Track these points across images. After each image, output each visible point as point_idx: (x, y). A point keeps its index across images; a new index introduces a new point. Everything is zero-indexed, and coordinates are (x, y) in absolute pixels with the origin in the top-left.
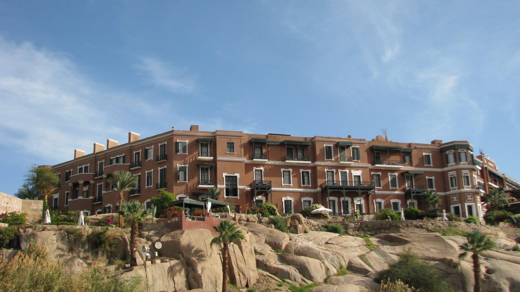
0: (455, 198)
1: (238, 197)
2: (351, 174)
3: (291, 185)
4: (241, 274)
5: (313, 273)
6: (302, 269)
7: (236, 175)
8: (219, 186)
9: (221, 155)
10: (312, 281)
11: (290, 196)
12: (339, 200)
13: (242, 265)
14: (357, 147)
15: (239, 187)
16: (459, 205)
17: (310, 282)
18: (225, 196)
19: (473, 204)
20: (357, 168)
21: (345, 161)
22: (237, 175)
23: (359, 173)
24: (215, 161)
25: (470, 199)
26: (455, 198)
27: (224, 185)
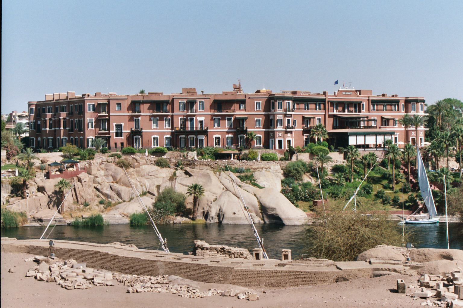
0: (272, 134)
1: (123, 137)
2: (196, 120)
3: (158, 128)
4: (81, 198)
5: (123, 195)
6: (118, 194)
7: (121, 124)
8: (111, 131)
9: (113, 112)
10: (121, 199)
11: (157, 135)
12: (187, 137)
13: (82, 194)
14: (203, 101)
15: (123, 131)
16: (273, 139)
17: (121, 201)
18: (115, 137)
19: (283, 139)
20: (201, 116)
21: (194, 112)
22: (123, 124)
23: (202, 119)
24: (109, 116)
25: (281, 136)
26: (272, 134)
27: (114, 130)
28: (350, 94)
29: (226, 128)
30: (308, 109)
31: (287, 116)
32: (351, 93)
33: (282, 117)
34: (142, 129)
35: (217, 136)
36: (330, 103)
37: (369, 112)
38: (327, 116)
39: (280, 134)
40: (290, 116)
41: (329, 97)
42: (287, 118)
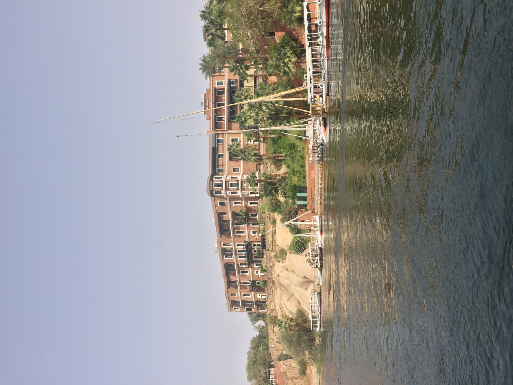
19: (249, 192)
28: (207, 103)
29: (245, 227)
30: (223, 155)
31: (227, 187)
32: (206, 99)
33: (229, 192)
34: (250, 281)
35: (251, 233)
36: (216, 130)
37: (225, 75)
38: (229, 132)
39: (244, 193)
40: (227, 183)
41: (211, 129)
42: (230, 187)
